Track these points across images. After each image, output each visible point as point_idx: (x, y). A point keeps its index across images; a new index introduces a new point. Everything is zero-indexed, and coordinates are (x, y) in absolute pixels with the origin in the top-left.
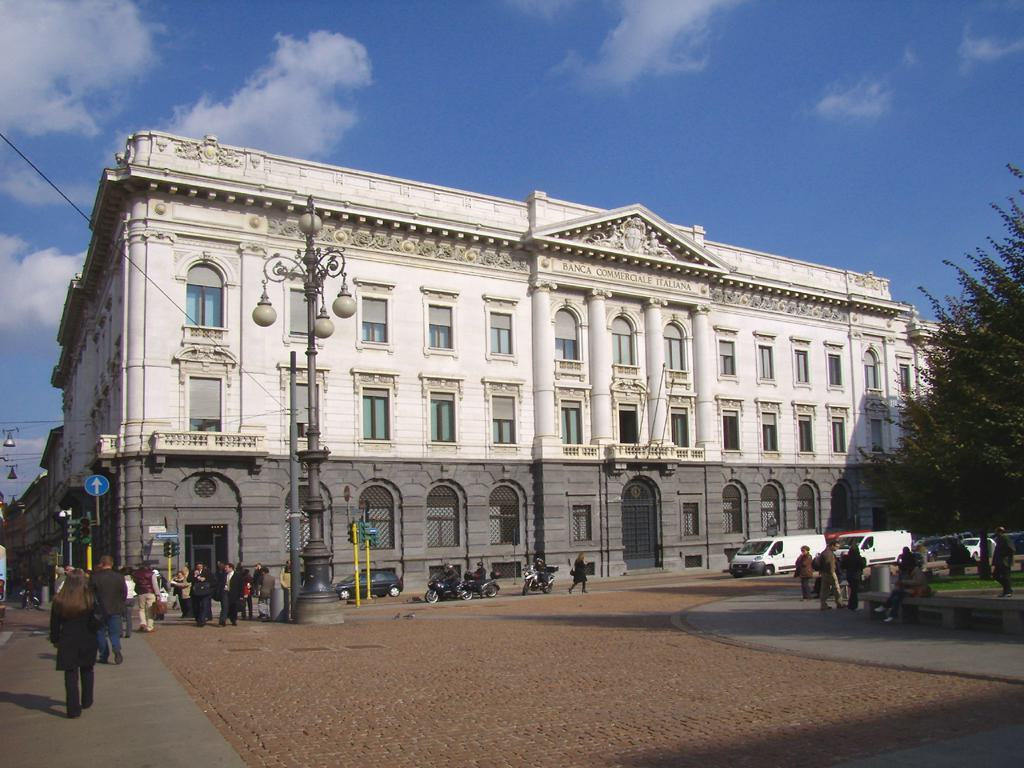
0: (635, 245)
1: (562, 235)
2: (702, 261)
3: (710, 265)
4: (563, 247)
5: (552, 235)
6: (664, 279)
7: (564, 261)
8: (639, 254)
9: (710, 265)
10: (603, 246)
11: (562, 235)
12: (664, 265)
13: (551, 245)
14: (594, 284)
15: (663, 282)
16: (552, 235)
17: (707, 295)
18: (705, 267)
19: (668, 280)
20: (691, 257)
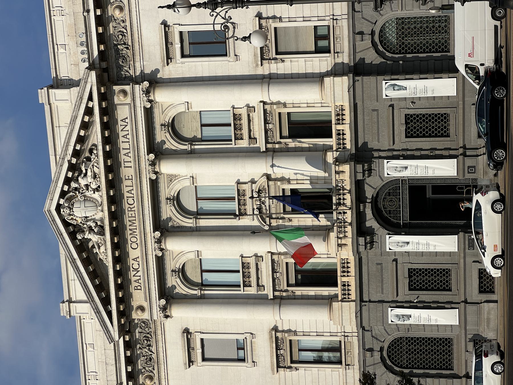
0: (90, 210)
1: (106, 302)
2: (89, 111)
3: (90, 98)
4: (120, 301)
5: (109, 314)
6: (123, 157)
7: (132, 289)
8: (101, 196)
9: (90, 98)
10: (105, 254)
11: (106, 302)
12: (109, 169)
13: (121, 314)
14: (150, 252)
15: (127, 159)
16: (109, 314)
17: (127, 88)
18: (95, 104)
19: (123, 152)
20: (85, 126)
